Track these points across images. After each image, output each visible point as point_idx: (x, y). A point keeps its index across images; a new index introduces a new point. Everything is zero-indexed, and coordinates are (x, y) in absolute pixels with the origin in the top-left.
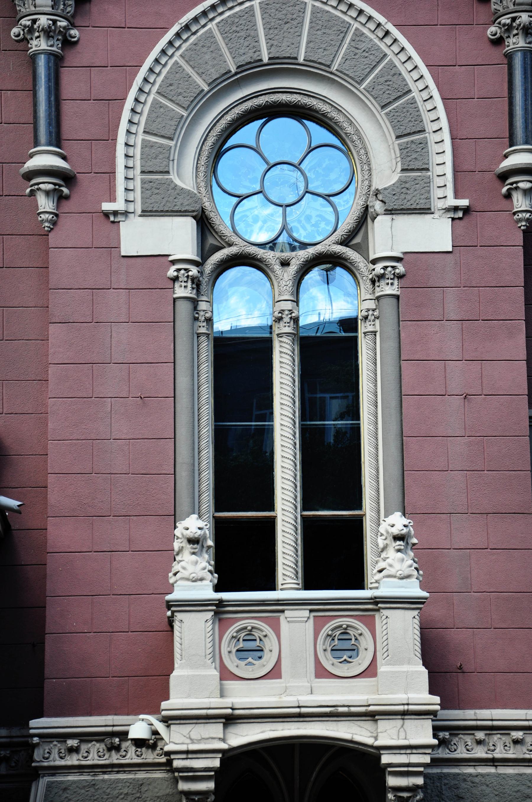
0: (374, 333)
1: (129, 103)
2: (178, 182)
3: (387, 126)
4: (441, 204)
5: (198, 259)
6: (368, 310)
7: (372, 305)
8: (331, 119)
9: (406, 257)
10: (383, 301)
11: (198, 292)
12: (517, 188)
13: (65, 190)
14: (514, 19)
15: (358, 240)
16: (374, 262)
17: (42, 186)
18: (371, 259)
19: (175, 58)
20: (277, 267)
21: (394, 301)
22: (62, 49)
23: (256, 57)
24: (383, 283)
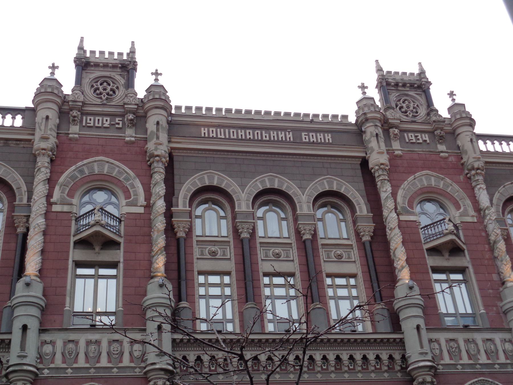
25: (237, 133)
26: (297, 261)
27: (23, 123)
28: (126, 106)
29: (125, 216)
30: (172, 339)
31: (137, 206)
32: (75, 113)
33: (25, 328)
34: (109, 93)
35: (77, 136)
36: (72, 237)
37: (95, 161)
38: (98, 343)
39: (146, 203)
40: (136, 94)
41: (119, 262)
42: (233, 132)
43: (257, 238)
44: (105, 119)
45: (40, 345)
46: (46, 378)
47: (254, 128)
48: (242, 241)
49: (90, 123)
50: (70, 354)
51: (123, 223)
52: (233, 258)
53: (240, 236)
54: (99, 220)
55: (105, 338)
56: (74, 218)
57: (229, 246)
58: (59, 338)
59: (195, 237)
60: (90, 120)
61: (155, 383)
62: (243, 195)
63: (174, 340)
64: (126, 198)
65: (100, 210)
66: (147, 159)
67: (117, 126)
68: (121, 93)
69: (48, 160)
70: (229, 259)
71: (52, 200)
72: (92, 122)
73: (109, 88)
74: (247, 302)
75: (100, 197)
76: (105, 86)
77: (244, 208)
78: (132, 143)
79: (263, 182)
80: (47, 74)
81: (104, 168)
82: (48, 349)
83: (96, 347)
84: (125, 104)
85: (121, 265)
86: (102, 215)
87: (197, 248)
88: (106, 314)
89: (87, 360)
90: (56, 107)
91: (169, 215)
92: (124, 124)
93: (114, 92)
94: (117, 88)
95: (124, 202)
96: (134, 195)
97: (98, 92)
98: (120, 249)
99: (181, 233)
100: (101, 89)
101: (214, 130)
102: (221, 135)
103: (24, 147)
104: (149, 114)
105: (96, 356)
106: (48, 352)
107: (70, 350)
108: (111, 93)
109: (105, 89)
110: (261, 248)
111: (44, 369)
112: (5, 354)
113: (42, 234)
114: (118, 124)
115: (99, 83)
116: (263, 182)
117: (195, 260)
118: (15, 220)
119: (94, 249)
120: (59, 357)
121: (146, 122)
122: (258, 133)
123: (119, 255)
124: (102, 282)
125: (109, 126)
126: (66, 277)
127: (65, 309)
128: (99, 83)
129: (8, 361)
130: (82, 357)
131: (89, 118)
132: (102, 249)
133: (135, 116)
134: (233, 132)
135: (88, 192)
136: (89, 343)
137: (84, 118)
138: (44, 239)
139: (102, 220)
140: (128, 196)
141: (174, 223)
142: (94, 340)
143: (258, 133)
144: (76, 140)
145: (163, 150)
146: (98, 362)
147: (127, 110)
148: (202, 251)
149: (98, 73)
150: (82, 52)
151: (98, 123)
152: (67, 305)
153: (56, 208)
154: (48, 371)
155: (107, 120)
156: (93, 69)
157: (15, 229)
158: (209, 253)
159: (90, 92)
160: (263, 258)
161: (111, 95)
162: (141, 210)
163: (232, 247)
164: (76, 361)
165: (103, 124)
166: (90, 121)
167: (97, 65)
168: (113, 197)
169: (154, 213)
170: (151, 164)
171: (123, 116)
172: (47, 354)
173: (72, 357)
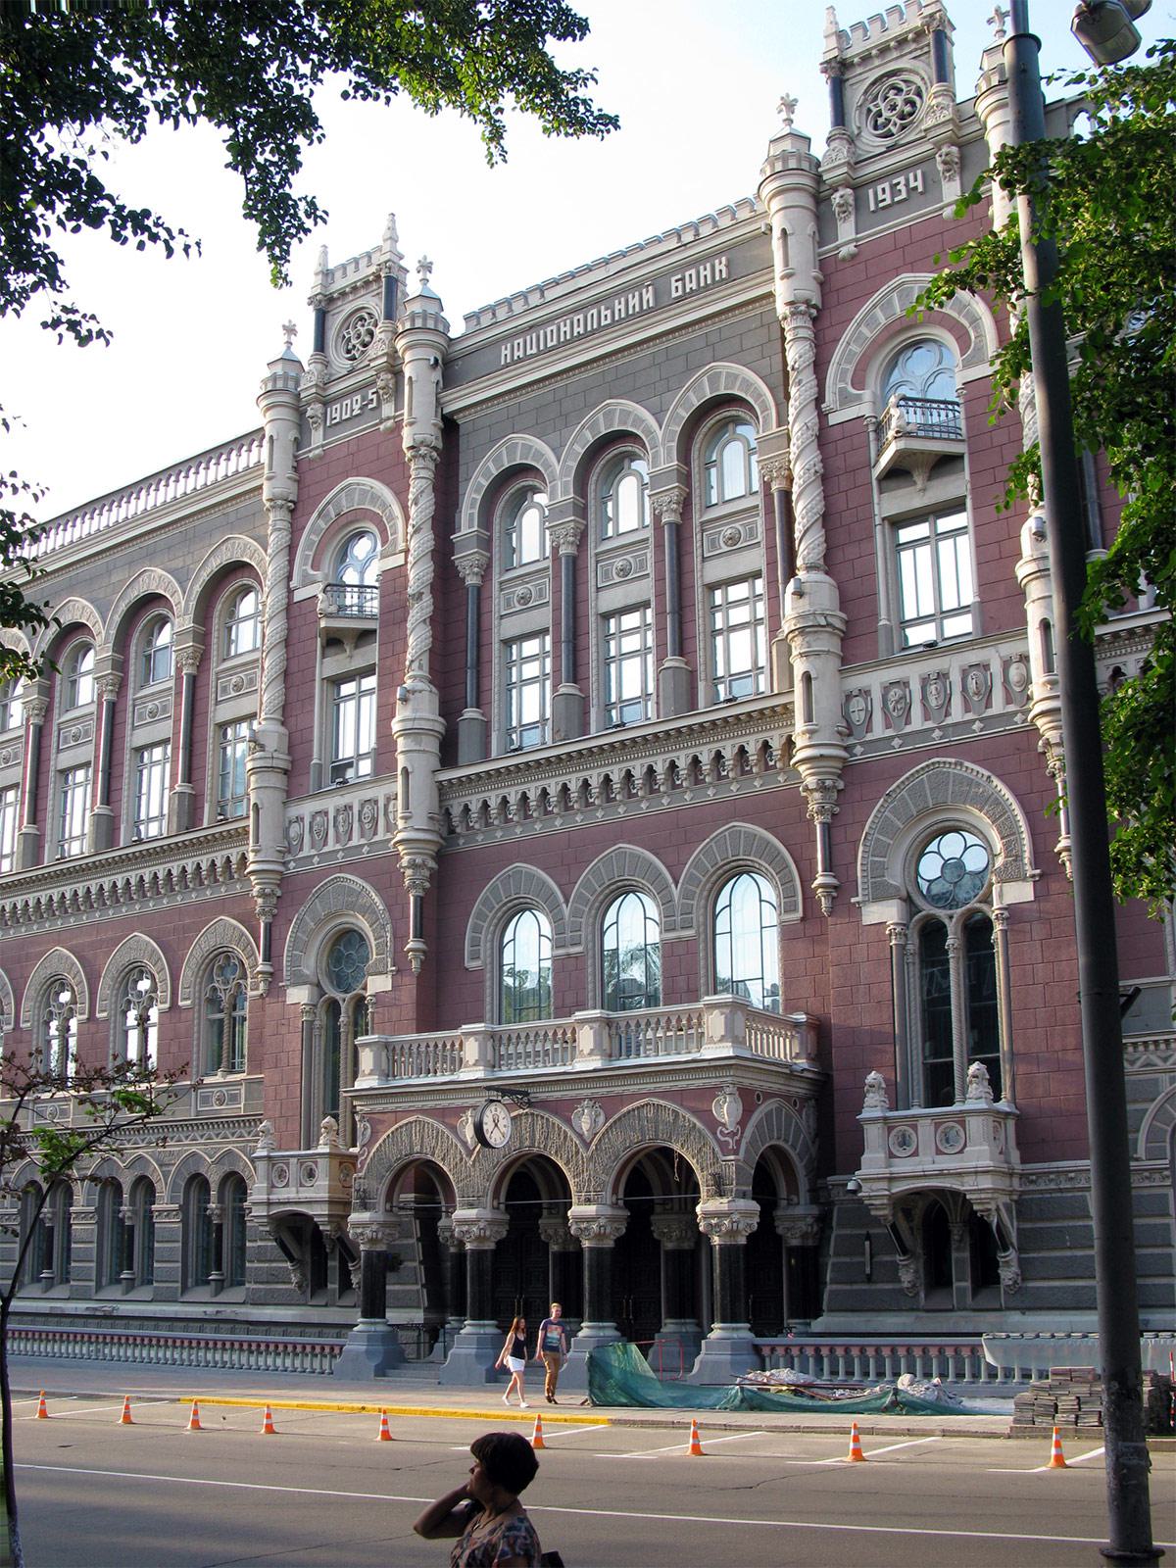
26: (652, 576)
28: (372, 365)
50: (318, 834)
55: (354, 798)
67: (370, 406)
69: (283, 514)
71: (293, 584)
72: (338, 415)
79: (593, 427)
93: (371, 334)
114: (372, 400)
117: (495, 622)
123: (371, 653)
126: (313, 711)
138: (287, 652)
141: (456, 562)
153: (298, 596)
156: (340, 303)
166: (337, 412)
167: (343, 294)
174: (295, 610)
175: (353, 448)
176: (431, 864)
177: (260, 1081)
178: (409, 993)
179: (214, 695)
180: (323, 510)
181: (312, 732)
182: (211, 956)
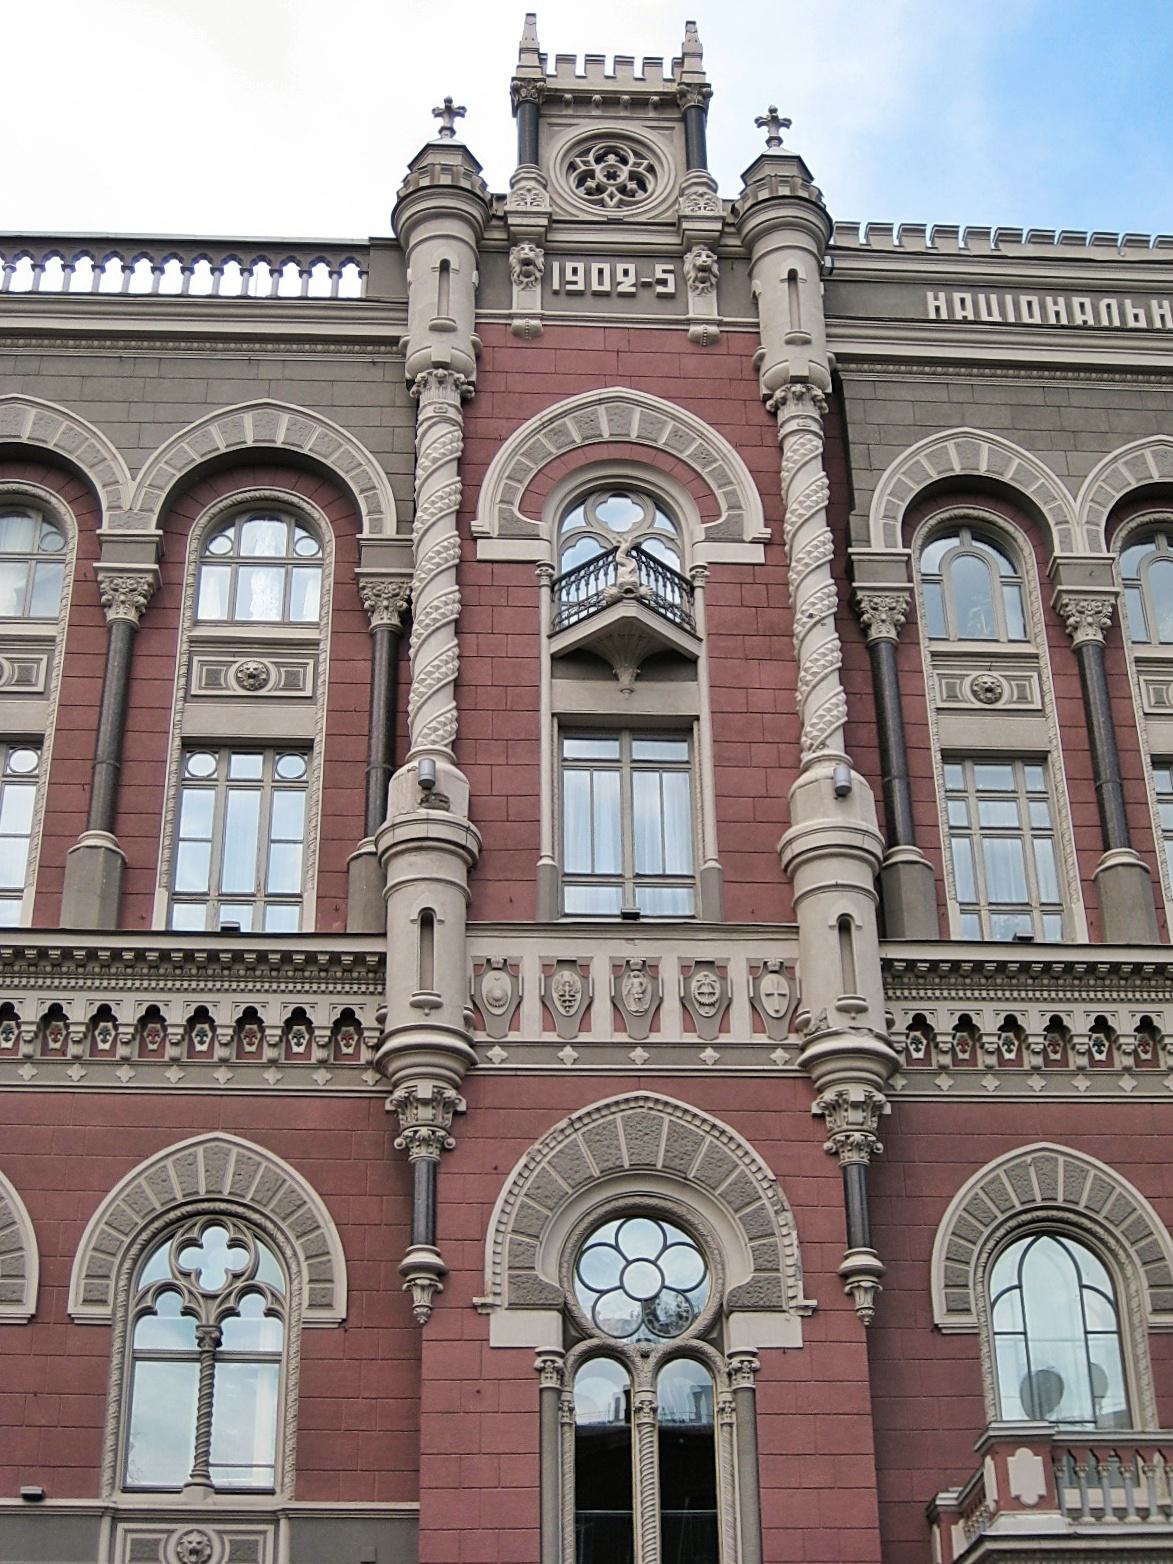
0: (730, 1425)
1: (499, 1203)
2: (542, 1277)
3: (740, 1229)
4: (793, 1303)
5: (563, 1351)
6: (725, 1402)
7: (728, 1397)
8: (687, 1221)
9: (760, 1352)
10: (740, 1395)
11: (562, 1384)
12: (859, 1287)
13: (440, 1286)
14: (848, 1137)
15: (714, 1335)
16: (731, 1356)
17: (418, 1281)
18: (727, 1352)
19: (543, 1164)
20: (638, 1359)
21: (749, 1395)
22: (440, 1155)
23: (618, 1163)
24: (739, 1375)
25: (1043, 307)
27: (367, 287)
28: (685, 225)
29: (707, 573)
30: (882, 959)
31: (744, 542)
32: (526, 250)
33: (427, 919)
34: (625, 186)
35: (536, 322)
36: (544, 640)
37: (600, 402)
38: (649, 968)
39: (769, 530)
40: (712, 186)
41: (697, 718)
42: (1030, 304)
43: (1127, 644)
44: (620, 268)
45: (470, 972)
46: (499, 1075)
47: (1097, 290)
48: (1078, 652)
49: (575, 283)
50: (567, 1002)
51: (698, 593)
52: (1052, 710)
53: (1070, 637)
54: (633, 583)
55: (669, 955)
56: (545, 581)
57: (1038, 670)
58: (531, 952)
59: (927, 643)
60: (575, 271)
61: (840, 1094)
62: (1076, 506)
63: (887, 965)
64: (704, 519)
65: (634, 553)
66: (764, 391)
67: (660, 289)
68: (661, 187)
70: (1040, 712)
71: (476, 526)
73: (624, 173)
74: (1107, 848)
75: (622, 516)
76: (611, 166)
77: (1081, 548)
78: (711, 341)
80: (430, 131)
81: (629, 423)
82: (495, 984)
83: (644, 981)
84: (680, 218)
85: (704, 731)
86: (640, 569)
87: (936, 678)
88: (664, 879)
89: (619, 1024)
90: (467, 234)
91: (843, 569)
92: (682, 280)
94: (651, 169)
95: (694, 527)
96: (730, 508)
97: (591, 184)
98: (695, 678)
99: (884, 628)
100: (600, 176)
101: (968, 297)
102: (990, 314)
103: (374, 363)
104: (761, 248)
105: (647, 1011)
106: (498, 993)
107: (567, 988)
108: (632, 185)
109: (612, 176)
110: (1142, 678)
111: (491, 1045)
112: (372, 1002)
113: (451, 628)
114: (664, 282)
115: (591, 157)
116: (1137, 464)
117: (931, 716)
118: (364, 588)
119: (616, 677)
120: (531, 1009)
121: (750, 275)
122: (1109, 306)
123: (693, 697)
124: (645, 781)
125: (633, 289)
127: (540, 863)
128: (591, 157)
129: (382, 1019)
130: (602, 1010)
131: (569, 266)
132: (638, 678)
133: (715, 258)
134: (1030, 304)
135: (580, 500)
136: (620, 969)
137: (556, 266)
139: (641, 585)
140: (709, 512)
141: (860, 595)
142: (636, 961)
143: (1109, 306)
144: (535, 334)
145: (813, 361)
146: (654, 1027)
147: (690, 238)
148: (951, 687)
149: (587, 126)
150: (534, 59)
151: (601, 283)
152: (546, 850)
153: (485, 550)
154: (504, 1054)
155: (626, 273)
156: (570, 112)
157: (366, 614)
158: (974, 693)
159: (564, 184)
160: (1147, 711)
161: (633, 194)
162: (757, 555)
163: (1047, 672)
164: (585, 1024)
165: (615, 283)
166: (576, 273)
167: (583, 100)
168: (659, 515)
169: (799, 560)
170: (777, 408)
171: (678, 256)
172: (497, 1002)
173: (572, 1011)
174: (473, 574)
175: (615, 341)
176: (887, 1110)
177: (413, 1517)
178: (853, 1361)
179: (183, 681)
180: (551, 421)
181: (537, 805)
182: (172, 1215)
